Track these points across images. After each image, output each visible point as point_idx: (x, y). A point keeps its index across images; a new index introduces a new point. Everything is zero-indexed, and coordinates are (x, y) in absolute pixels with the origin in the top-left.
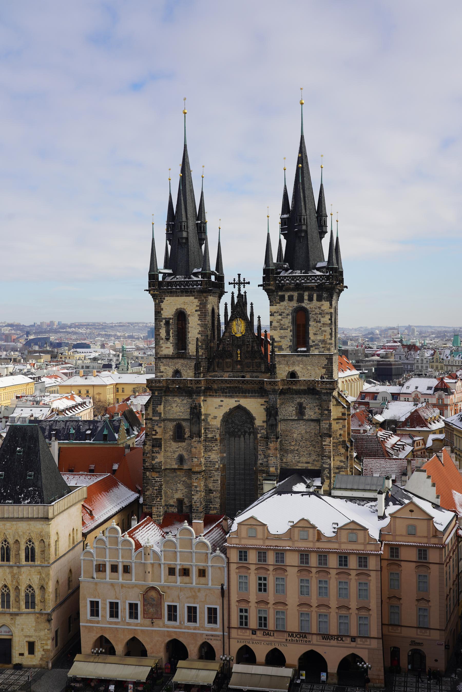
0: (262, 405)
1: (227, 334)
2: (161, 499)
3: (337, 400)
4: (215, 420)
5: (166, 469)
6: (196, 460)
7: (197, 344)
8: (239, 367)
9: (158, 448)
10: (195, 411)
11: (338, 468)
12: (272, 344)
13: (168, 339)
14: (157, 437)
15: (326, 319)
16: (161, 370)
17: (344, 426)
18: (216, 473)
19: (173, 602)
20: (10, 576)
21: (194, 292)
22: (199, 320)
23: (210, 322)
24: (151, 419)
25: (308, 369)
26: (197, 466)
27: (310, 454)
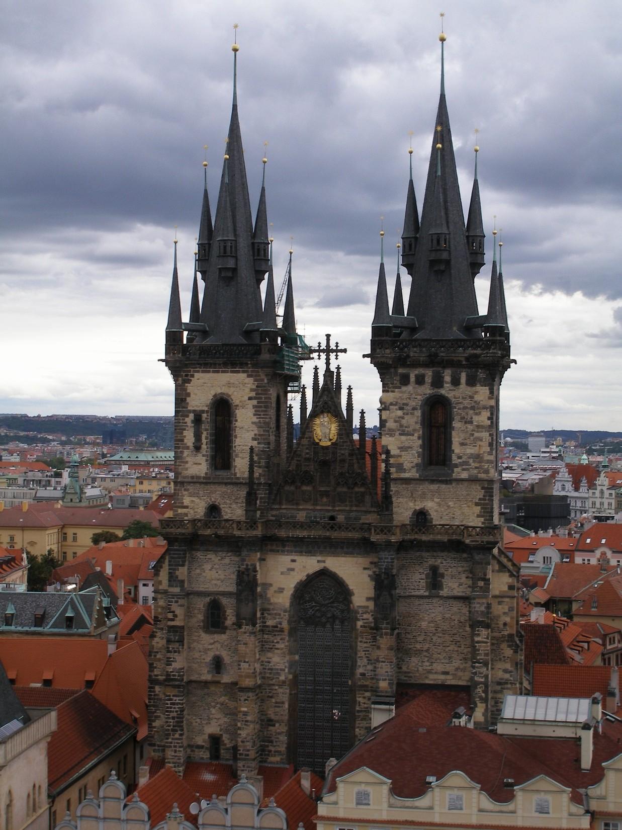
0: (365, 569)
1: (305, 442)
2: (181, 735)
3: (500, 562)
4: (281, 595)
5: (190, 682)
6: (244, 665)
8: (325, 499)
9: (177, 644)
10: (246, 578)
11: (499, 683)
12: (386, 461)
13: (197, 448)
14: (177, 623)
15: (483, 418)
16: (185, 504)
17: (511, 609)
18: (281, 690)
22: (255, 415)
23: (274, 418)
24: (165, 592)
25: (449, 507)
26: (248, 676)
27: (450, 658)
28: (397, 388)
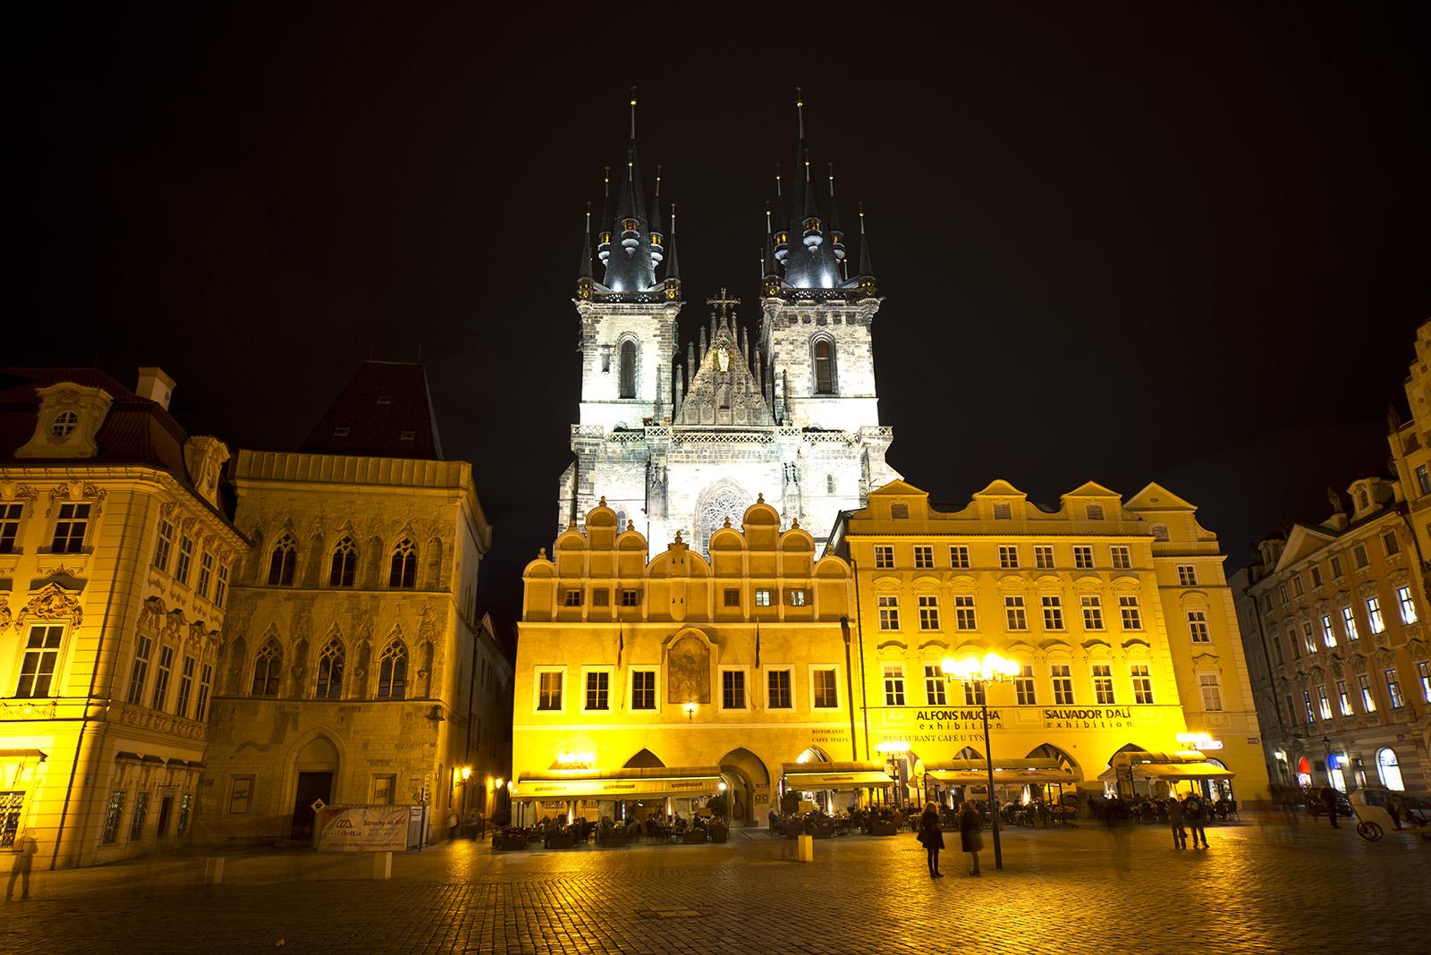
7: (659, 379)
8: (725, 419)
19: (736, 662)
20: (349, 616)
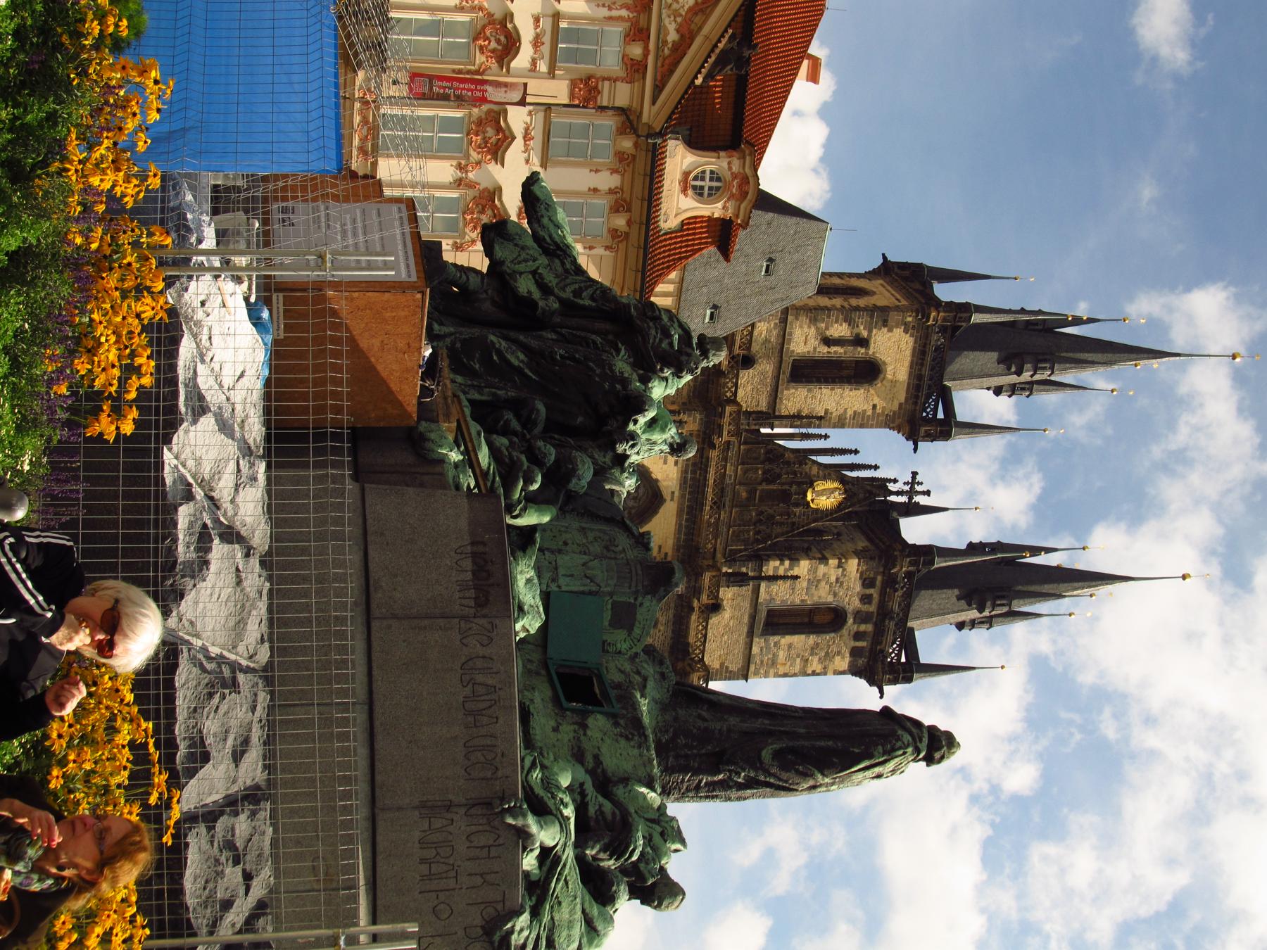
0: (660, 547)
1: (815, 470)
13: (827, 341)
21: (916, 403)
28: (862, 574)
